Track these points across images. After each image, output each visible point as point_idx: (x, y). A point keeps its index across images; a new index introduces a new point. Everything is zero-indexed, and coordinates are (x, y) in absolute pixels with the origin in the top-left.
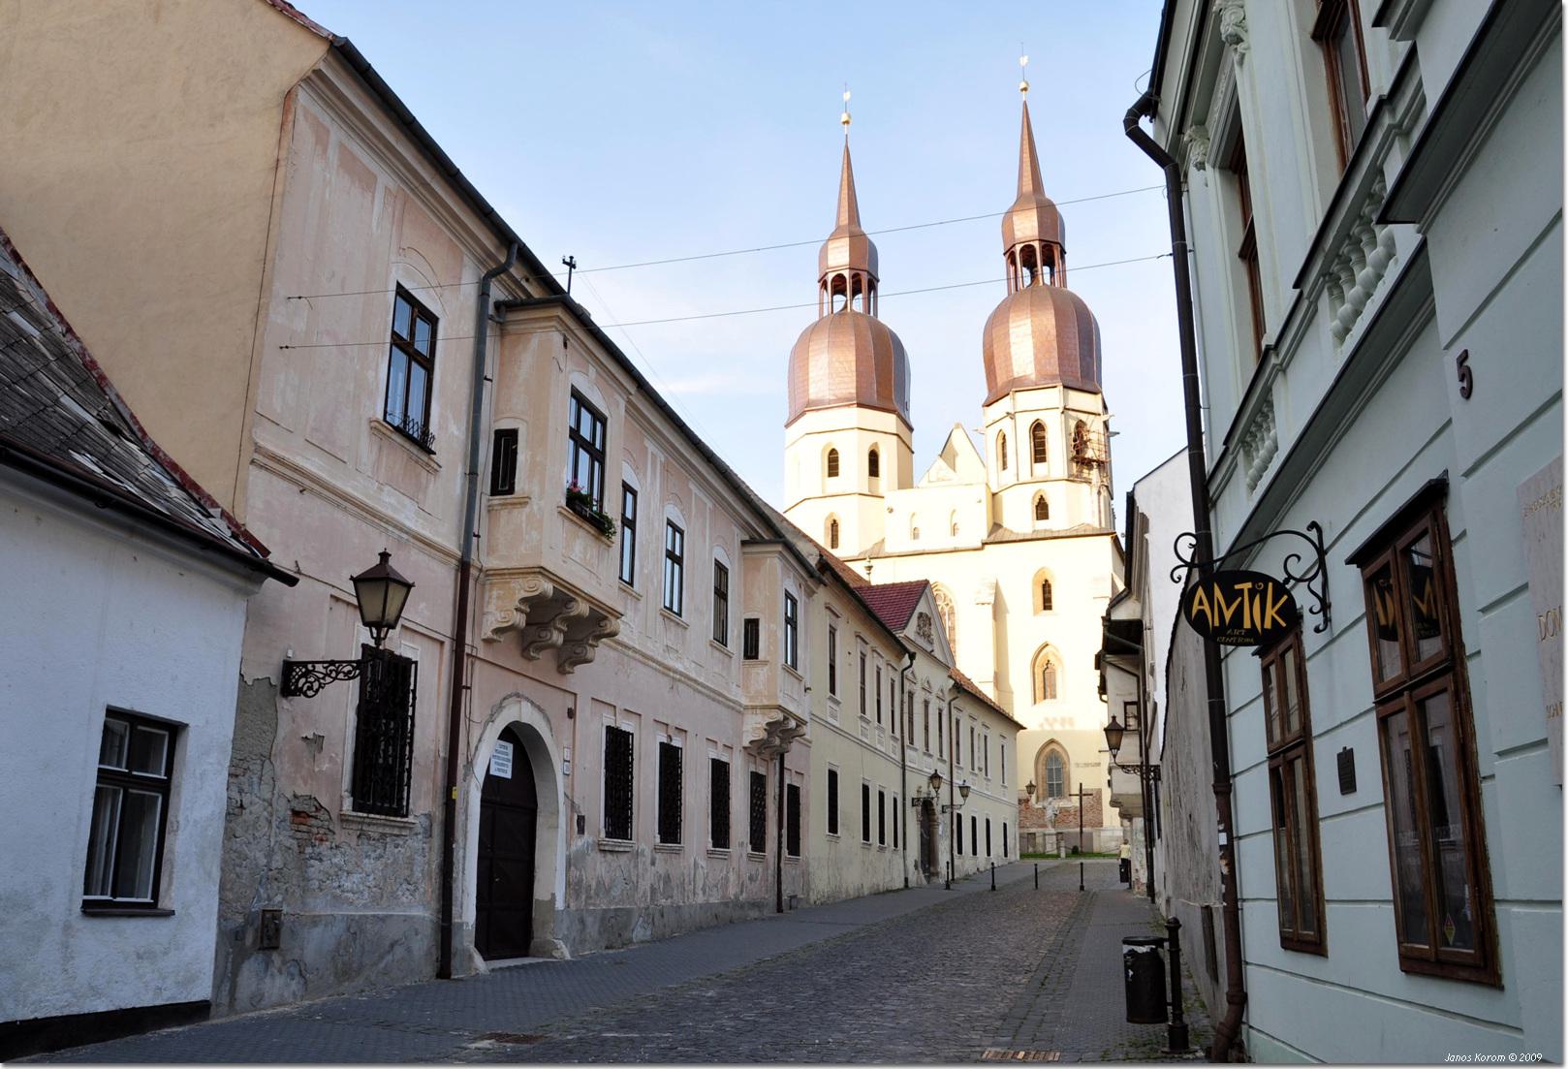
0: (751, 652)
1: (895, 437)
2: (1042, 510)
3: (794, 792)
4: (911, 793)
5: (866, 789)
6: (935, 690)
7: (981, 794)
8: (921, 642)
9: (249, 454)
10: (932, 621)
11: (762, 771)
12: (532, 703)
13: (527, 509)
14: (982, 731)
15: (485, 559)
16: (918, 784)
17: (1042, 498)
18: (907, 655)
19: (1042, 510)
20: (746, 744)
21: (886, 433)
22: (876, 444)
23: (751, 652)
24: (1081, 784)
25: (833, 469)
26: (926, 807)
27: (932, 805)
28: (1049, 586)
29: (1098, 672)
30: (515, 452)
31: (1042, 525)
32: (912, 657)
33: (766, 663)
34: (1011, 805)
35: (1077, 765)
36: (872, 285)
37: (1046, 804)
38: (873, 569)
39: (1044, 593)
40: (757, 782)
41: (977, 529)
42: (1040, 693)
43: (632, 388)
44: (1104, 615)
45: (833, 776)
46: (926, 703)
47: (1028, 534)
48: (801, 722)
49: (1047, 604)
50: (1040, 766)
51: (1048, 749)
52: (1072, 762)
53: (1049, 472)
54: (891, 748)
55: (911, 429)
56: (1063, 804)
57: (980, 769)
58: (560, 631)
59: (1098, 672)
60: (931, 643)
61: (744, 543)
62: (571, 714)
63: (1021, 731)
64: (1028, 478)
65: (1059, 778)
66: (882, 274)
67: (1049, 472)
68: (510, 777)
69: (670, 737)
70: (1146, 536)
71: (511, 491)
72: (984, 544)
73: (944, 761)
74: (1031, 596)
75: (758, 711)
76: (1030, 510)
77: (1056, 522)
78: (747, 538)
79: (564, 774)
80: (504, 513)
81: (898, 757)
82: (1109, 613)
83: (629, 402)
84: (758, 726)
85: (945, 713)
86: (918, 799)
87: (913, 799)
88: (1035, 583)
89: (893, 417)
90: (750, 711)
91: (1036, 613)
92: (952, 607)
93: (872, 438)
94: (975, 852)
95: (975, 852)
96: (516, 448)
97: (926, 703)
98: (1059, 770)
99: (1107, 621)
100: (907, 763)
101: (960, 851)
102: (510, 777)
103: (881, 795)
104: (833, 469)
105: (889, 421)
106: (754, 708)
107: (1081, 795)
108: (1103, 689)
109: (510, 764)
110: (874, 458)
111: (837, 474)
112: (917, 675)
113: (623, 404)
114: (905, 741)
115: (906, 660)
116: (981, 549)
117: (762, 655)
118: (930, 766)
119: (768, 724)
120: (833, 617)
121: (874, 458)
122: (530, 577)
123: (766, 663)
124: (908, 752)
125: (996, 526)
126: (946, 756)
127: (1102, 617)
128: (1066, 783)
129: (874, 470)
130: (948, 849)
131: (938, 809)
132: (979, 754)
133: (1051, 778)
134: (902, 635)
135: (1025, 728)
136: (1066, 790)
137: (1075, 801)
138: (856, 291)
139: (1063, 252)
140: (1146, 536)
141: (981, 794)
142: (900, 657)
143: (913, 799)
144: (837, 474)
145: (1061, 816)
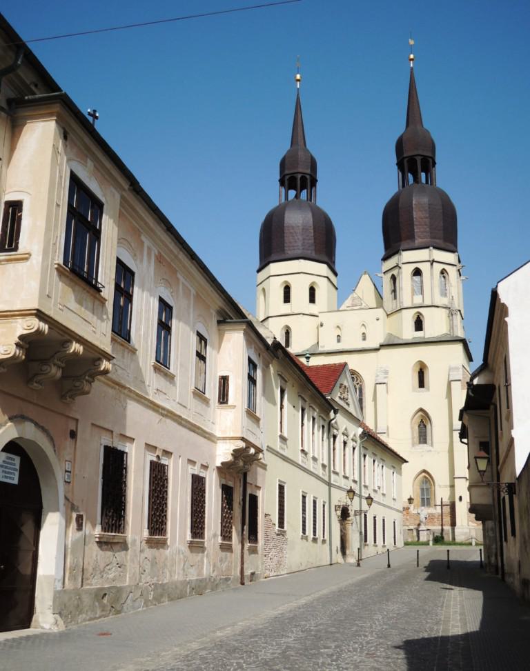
0: (223, 399)
1: (326, 279)
2: (419, 325)
3: (254, 499)
4: (335, 502)
5: (304, 497)
6: (351, 436)
7: (379, 504)
8: (342, 403)
11: (230, 484)
12: (36, 424)
13: (28, 263)
16: (340, 498)
17: (418, 318)
18: (332, 411)
19: (419, 325)
20: (219, 464)
21: (320, 276)
22: (313, 283)
23: (223, 399)
25: (287, 299)
26: (345, 514)
27: (348, 510)
29: (461, 422)
30: (20, 218)
31: (419, 334)
33: (234, 407)
35: (440, 486)
36: (314, 182)
37: (419, 512)
42: (417, 440)
43: (126, 186)
45: (281, 488)
46: (345, 443)
47: (409, 340)
48: (259, 450)
49: (422, 384)
56: (431, 510)
57: (379, 488)
58: (59, 367)
59: (461, 422)
61: (219, 322)
62: (73, 435)
63: (405, 464)
64: (410, 305)
65: (428, 494)
66: (319, 176)
68: (15, 482)
69: (158, 457)
70: (506, 319)
71: (16, 249)
72: (382, 346)
75: (228, 441)
77: (430, 331)
78: (221, 319)
79: (65, 481)
80: (10, 266)
82: (472, 379)
83: (122, 197)
84: (228, 451)
86: (339, 506)
89: (325, 266)
90: (222, 441)
91: (414, 390)
93: (311, 279)
96: (21, 215)
97: (345, 443)
99: (470, 385)
102: (15, 482)
103: (315, 502)
104: (287, 299)
105: (323, 269)
106: (224, 439)
109: (17, 474)
111: (289, 302)
112: (339, 423)
113: (118, 197)
115: (332, 414)
116: (377, 350)
120: (283, 382)
122: (28, 318)
127: (467, 383)
131: (351, 513)
133: (423, 494)
134: (329, 398)
135: (407, 462)
138: (303, 188)
139: (434, 163)
140: (506, 319)
141: (379, 504)
143: (336, 506)
144: (289, 302)
145: (430, 518)
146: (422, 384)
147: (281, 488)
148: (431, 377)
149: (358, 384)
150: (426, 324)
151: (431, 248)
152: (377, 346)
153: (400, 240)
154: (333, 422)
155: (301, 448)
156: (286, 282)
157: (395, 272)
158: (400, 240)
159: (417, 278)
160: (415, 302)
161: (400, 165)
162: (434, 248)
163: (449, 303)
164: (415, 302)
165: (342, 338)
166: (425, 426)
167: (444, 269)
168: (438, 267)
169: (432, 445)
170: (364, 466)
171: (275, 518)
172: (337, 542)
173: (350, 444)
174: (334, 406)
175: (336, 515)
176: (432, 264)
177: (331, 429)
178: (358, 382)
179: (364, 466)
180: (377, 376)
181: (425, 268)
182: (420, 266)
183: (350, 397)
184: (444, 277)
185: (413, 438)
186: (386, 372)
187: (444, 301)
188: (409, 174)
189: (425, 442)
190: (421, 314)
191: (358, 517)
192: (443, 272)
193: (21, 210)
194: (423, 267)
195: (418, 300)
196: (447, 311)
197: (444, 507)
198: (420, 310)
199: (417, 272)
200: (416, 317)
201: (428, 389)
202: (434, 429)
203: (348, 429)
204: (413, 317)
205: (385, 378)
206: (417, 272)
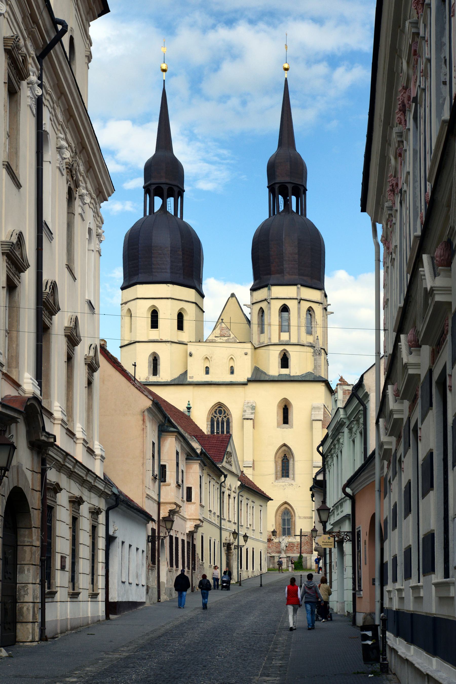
0: (189, 499)
5: (210, 540)
6: (233, 489)
7: (253, 539)
8: (228, 466)
9: (145, 495)
10: (232, 454)
13: (170, 486)
14: (250, 504)
15: (162, 500)
18: (223, 476)
20: (188, 532)
23: (189, 499)
24: (301, 529)
26: (228, 546)
31: (285, 371)
32: (225, 476)
33: (194, 503)
34: (263, 542)
35: (300, 517)
37: (281, 540)
38: (191, 410)
40: (188, 543)
42: (280, 474)
43: (182, 440)
44: (314, 477)
45: (202, 537)
46: (229, 495)
49: (286, 420)
50: (278, 517)
51: (283, 507)
52: (297, 515)
53: (290, 338)
54: (217, 522)
55: (203, 296)
57: (250, 525)
60: (231, 465)
61: (186, 459)
65: (289, 525)
67: (290, 338)
71: (165, 481)
72: (249, 381)
75: (192, 520)
81: (219, 525)
82: (316, 477)
83: (182, 445)
87: (224, 543)
88: (278, 406)
89: (193, 291)
90: (189, 520)
91: (278, 426)
92: (228, 419)
94: (247, 569)
95: (247, 569)
97: (229, 495)
100: (222, 527)
101: (241, 568)
106: (190, 519)
107: (301, 536)
108: (313, 496)
110: (180, 317)
115: (222, 478)
117: (193, 500)
118: (234, 528)
119: (195, 525)
121: (180, 317)
122: (172, 504)
123: (194, 503)
124: (222, 521)
125: (256, 370)
127: (313, 478)
129: (180, 327)
130: (236, 567)
131: (233, 547)
133: (284, 524)
134: (221, 466)
137: (298, 539)
139: (305, 190)
141: (253, 539)
142: (219, 477)
143: (224, 543)
145: (290, 547)
146: (286, 420)
147: (202, 537)
148: (295, 415)
149: (225, 417)
150: (292, 361)
151: (299, 286)
152: (244, 380)
153: (269, 273)
154: (223, 484)
155: (209, 509)
156: (154, 306)
158: (270, 274)
159: (285, 314)
160: (282, 339)
161: (271, 188)
162: (302, 285)
163: (314, 341)
164: (282, 339)
165: (211, 371)
166: (288, 461)
167: (310, 307)
168: (305, 306)
169: (294, 479)
170: (241, 510)
171: (200, 558)
173: (233, 495)
174: (223, 471)
176: (299, 302)
177: (222, 488)
178: (226, 414)
179: (241, 510)
180: (245, 411)
181: (292, 305)
182: (288, 303)
183: (232, 460)
184: (311, 315)
185: (276, 472)
186: (253, 408)
187: (310, 339)
188: (280, 197)
189: (288, 476)
190: (287, 351)
191: (236, 550)
192: (310, 310)
193: (165, 468)
195: (285, 337)
196: (311, 350)
197: (303, 537)
198: (288, 348)
199: (285, 309)
200: (282, 354)
201: (292, 427)
203: (231, 485)
204: (280, 354)
205: (252, 413)
206: (285, 309)
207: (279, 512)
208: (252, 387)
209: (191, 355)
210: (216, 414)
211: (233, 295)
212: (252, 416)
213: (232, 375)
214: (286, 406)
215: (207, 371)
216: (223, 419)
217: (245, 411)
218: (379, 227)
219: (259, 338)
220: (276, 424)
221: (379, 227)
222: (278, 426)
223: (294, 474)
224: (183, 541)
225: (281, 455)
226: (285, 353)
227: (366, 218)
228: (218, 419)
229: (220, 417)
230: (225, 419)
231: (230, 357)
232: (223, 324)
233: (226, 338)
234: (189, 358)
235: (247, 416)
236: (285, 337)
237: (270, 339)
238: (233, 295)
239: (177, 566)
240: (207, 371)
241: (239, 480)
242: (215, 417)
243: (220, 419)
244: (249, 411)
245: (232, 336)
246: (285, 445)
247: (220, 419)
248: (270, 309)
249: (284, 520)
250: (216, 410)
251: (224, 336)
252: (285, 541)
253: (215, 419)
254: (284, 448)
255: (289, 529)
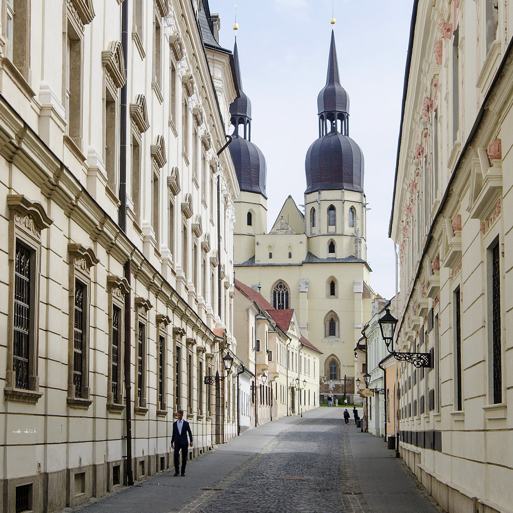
2: (332, 248)
4: (289, 385)
6: (295, 348)
14: (306, 356)
18: (289, 339)
19: (332, 248)
22: (251, 209)
28: (334, 284)
31: (332, 255)
32: (291, 340)
39: (331, 287)
41: (300, 256)
42: (328, 333)
47: (324, 260)
49: (333, 292)
50: (326, 365)
51: (331, 358)
52: (341, 364)
56: (337, 382)
64: (326, 233)
73: (297, 372)
74: (325, 289)
76: (326, 248)
85: (298, 355)
88: (327, 282)
91: (327, 297)
92: (287, 292)
98: (335, 368)
101: (301, 404)
107: (345, 380)
114: (288, 368)
116: (301, 265)
118: (296, 376)
123: (273, 362)
125: (310, 254)
126: (298, 371)
128: (339, 373)
131: (295, 389)
132: (307, 367)
133: (331, 371)
136: (338, 377)
137: (343, 382)
146: (333, 292)
148: (340, 289)
149: (285, 290)
150: (337, 249)
152: (299, 262)
157: (315, 206)
166: (335, 324)
169: (339, 337)
171: (275, 398)
172: (290, 405)
175: (290, 391)
194: (336, 204)
197: (347, 381)
198: (334, 238)
200: (330, 242)
201: (337, 298)
202: (341, 325)
204: (328, 242)
205: (306, 288)
207: (328, 362)
208: (306, 267)
209: (258, 244)
210: (278, 288)
211: (290, 197)
212: (307, 290)
213: (290, 259)
214: (333, 282)
215: (271, 256)
216: (283, 291)
217: (300, 286)
218: (398, 246)
219: (311, 229)
220: (324, 295)
221: (398, 246)
222: (327, 297)
223: (339, 333)
224: (266, 387)
225: (329, 318)
226: (332, 242)
227: (391, 241)
228: (279, 292)
229: (281, 290)
230: (285, 292)
231: (288, 246)
232: (282, 220)
233: (286, 231)
234: (256, 246)
235: (302, 290)
236: (332, 229)
237: (320, 231)
238: (290, 197)
239: (264, 404)
240: (271, 256)
241: (299, 341)
242: (277, 290)
243: (281, 292)
244: (303, 286)
245: (290, 229)
246: (332, 311)
247: (281, 292)
248: (320, 208)
249: (331, 368)
250: (278, 285)
251: (284, 229)
252: (332, 384)
253: (277, 292)
254: (331, 313)
255: (335, 375)
